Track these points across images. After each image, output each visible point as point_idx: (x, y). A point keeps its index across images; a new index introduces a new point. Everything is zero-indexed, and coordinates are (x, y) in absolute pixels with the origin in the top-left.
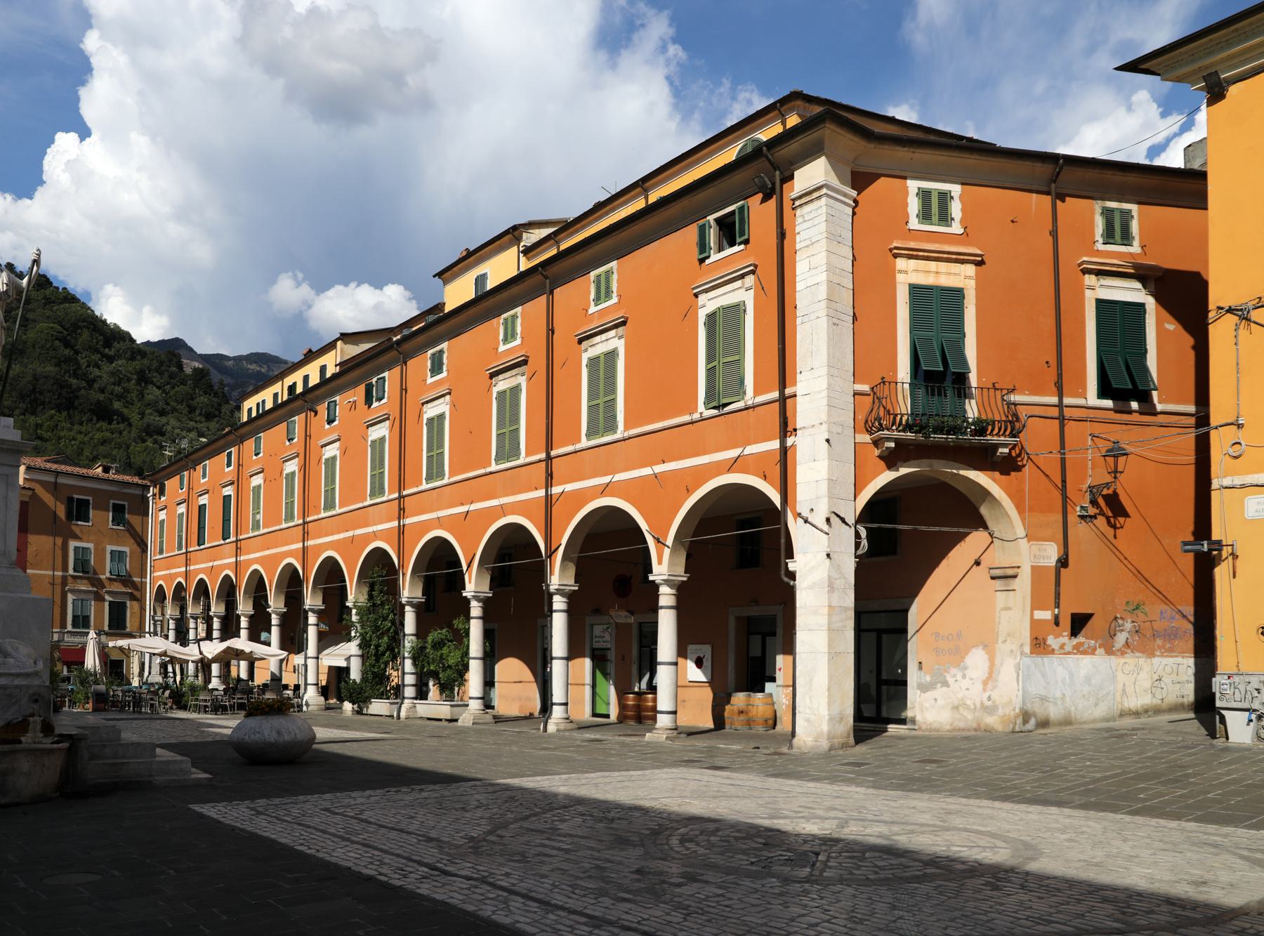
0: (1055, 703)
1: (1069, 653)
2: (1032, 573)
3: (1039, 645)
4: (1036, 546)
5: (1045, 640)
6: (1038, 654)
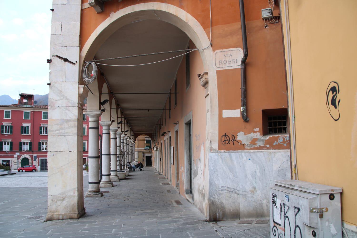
0: (245, 196)
1: (261, 148)
2: (218, 78)
3: (228, 141)
4: (220, 54)
5: (234, 137)
6: (227, 149)
